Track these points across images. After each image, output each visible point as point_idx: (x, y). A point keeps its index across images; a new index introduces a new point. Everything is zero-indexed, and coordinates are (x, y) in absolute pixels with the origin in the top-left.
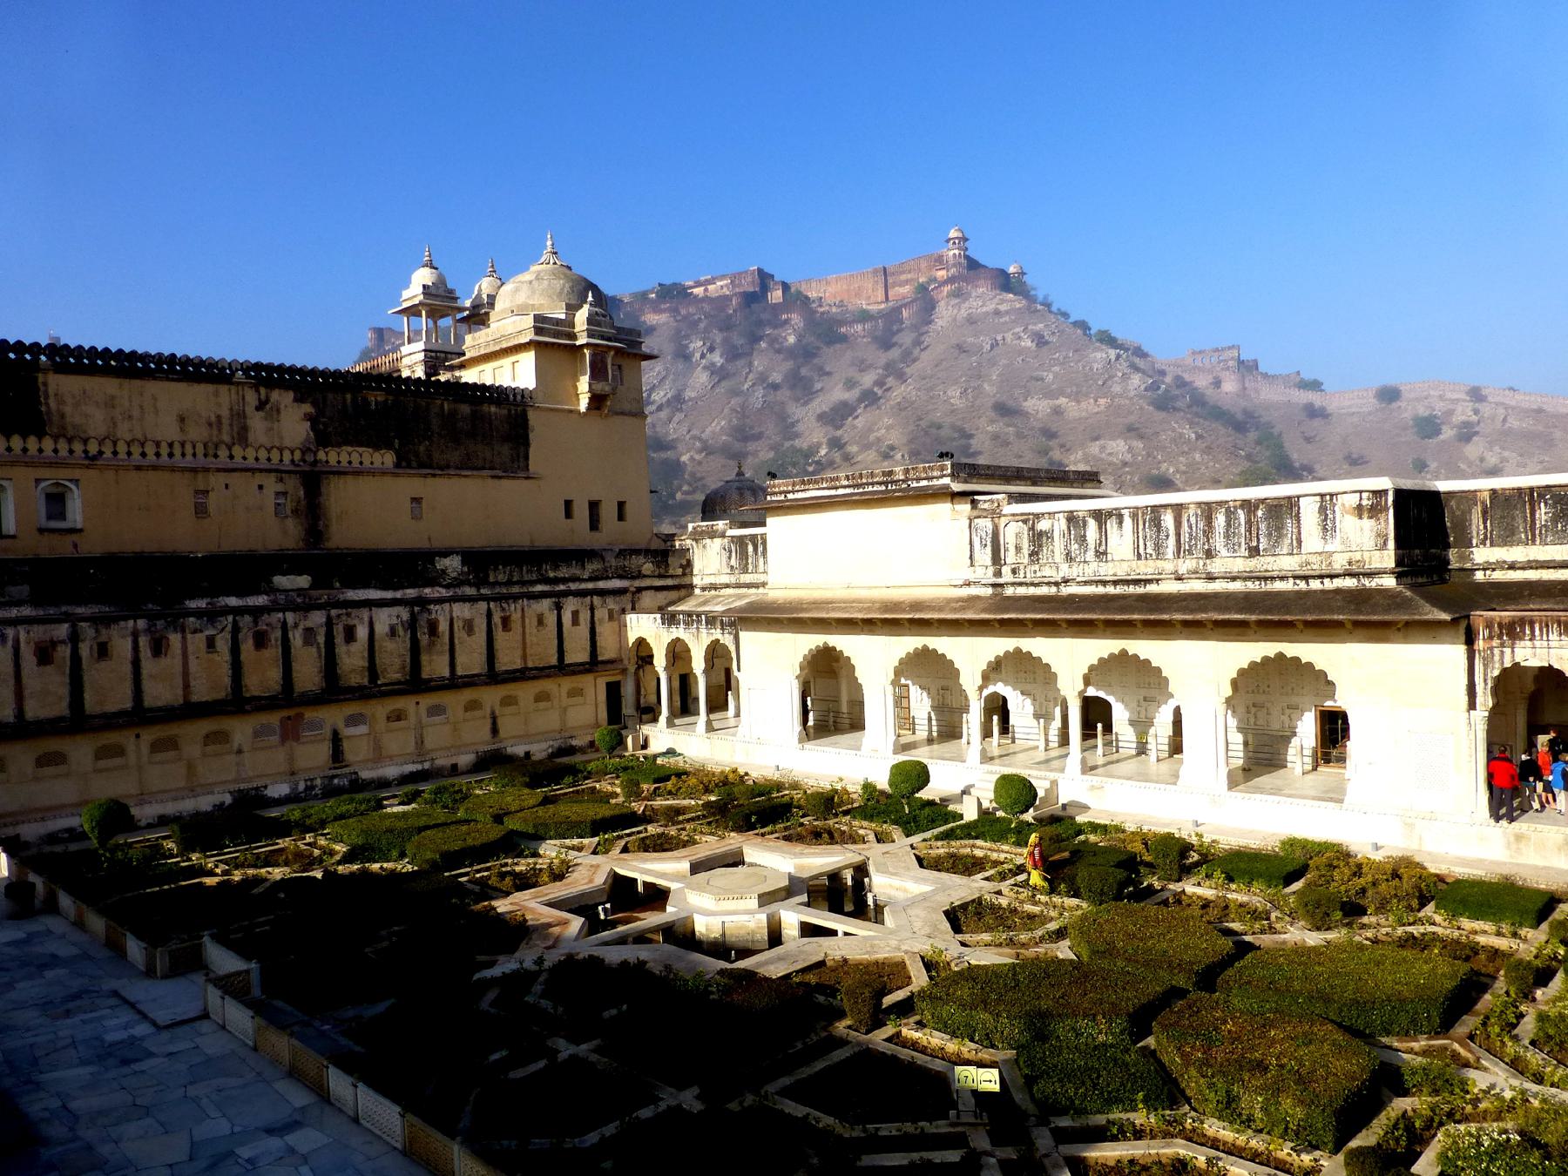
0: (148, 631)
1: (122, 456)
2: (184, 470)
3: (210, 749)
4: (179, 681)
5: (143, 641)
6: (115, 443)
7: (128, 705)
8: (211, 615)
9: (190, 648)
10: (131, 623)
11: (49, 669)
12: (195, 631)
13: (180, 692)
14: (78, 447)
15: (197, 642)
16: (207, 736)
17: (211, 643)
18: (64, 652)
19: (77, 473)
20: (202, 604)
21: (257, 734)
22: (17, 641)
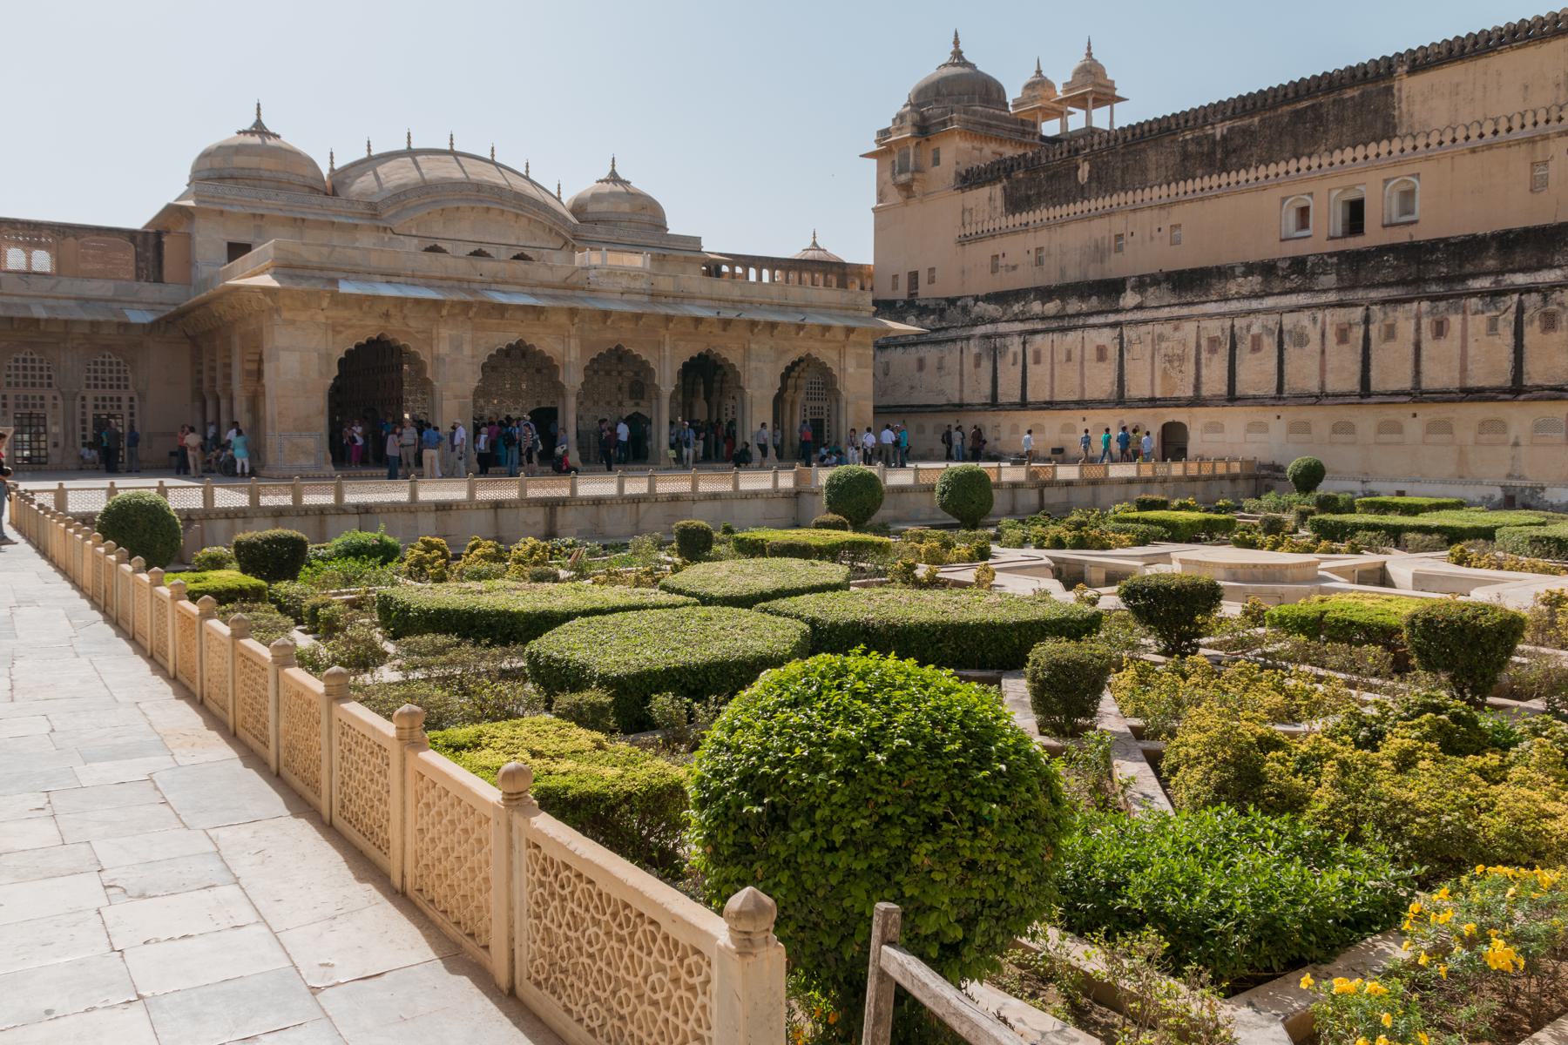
0: (1431, 313)
1: (1461, 139)
2: (1519, 143)
3: (1484, 437)
4: (1456, 363)
5: (1426, 322)
6: (1454, 130)
7: (1407, 384)
8: (1496, 294)
9: (1470, 331)
10: (1415, 304)
11: (1345, 347)
12: (1476, 313)
13: (1457, 375)
14: (1421, 142)
15: (1478, 323)
16: (1482, 424)
17: (1493, 327)
18: (1358, 332)
19: (1416, 168)
20: (1485, 283)
21: (1538, 427)
22: (1324, 323)
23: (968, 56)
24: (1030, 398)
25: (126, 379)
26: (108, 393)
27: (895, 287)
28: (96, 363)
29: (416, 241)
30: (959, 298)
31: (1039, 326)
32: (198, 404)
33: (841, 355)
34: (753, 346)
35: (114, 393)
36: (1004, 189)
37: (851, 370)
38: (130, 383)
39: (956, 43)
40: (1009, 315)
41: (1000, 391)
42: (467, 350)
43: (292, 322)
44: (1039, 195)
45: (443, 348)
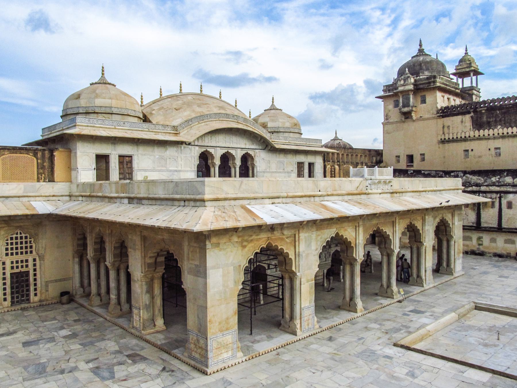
23: (426, 51)
24: (504, 225)
25: (31, 247)
26: (20, 257)
27: (398, 161)
28: (12, 239)
29: (197, 148)
30: (453, 172)
31: (511, 189)
32: (77, 260)
33: (453, 216)
34: (427, 217)
35: (23, 257)
36: (472, 117)
37: (456, 224)
38: (34, 249)
39: (421, 45)
40: (489, 181)
41: (482, 220)
42: (313, 247)
43: (218, 245)
44: (496, 121)
45: (302, 247)
